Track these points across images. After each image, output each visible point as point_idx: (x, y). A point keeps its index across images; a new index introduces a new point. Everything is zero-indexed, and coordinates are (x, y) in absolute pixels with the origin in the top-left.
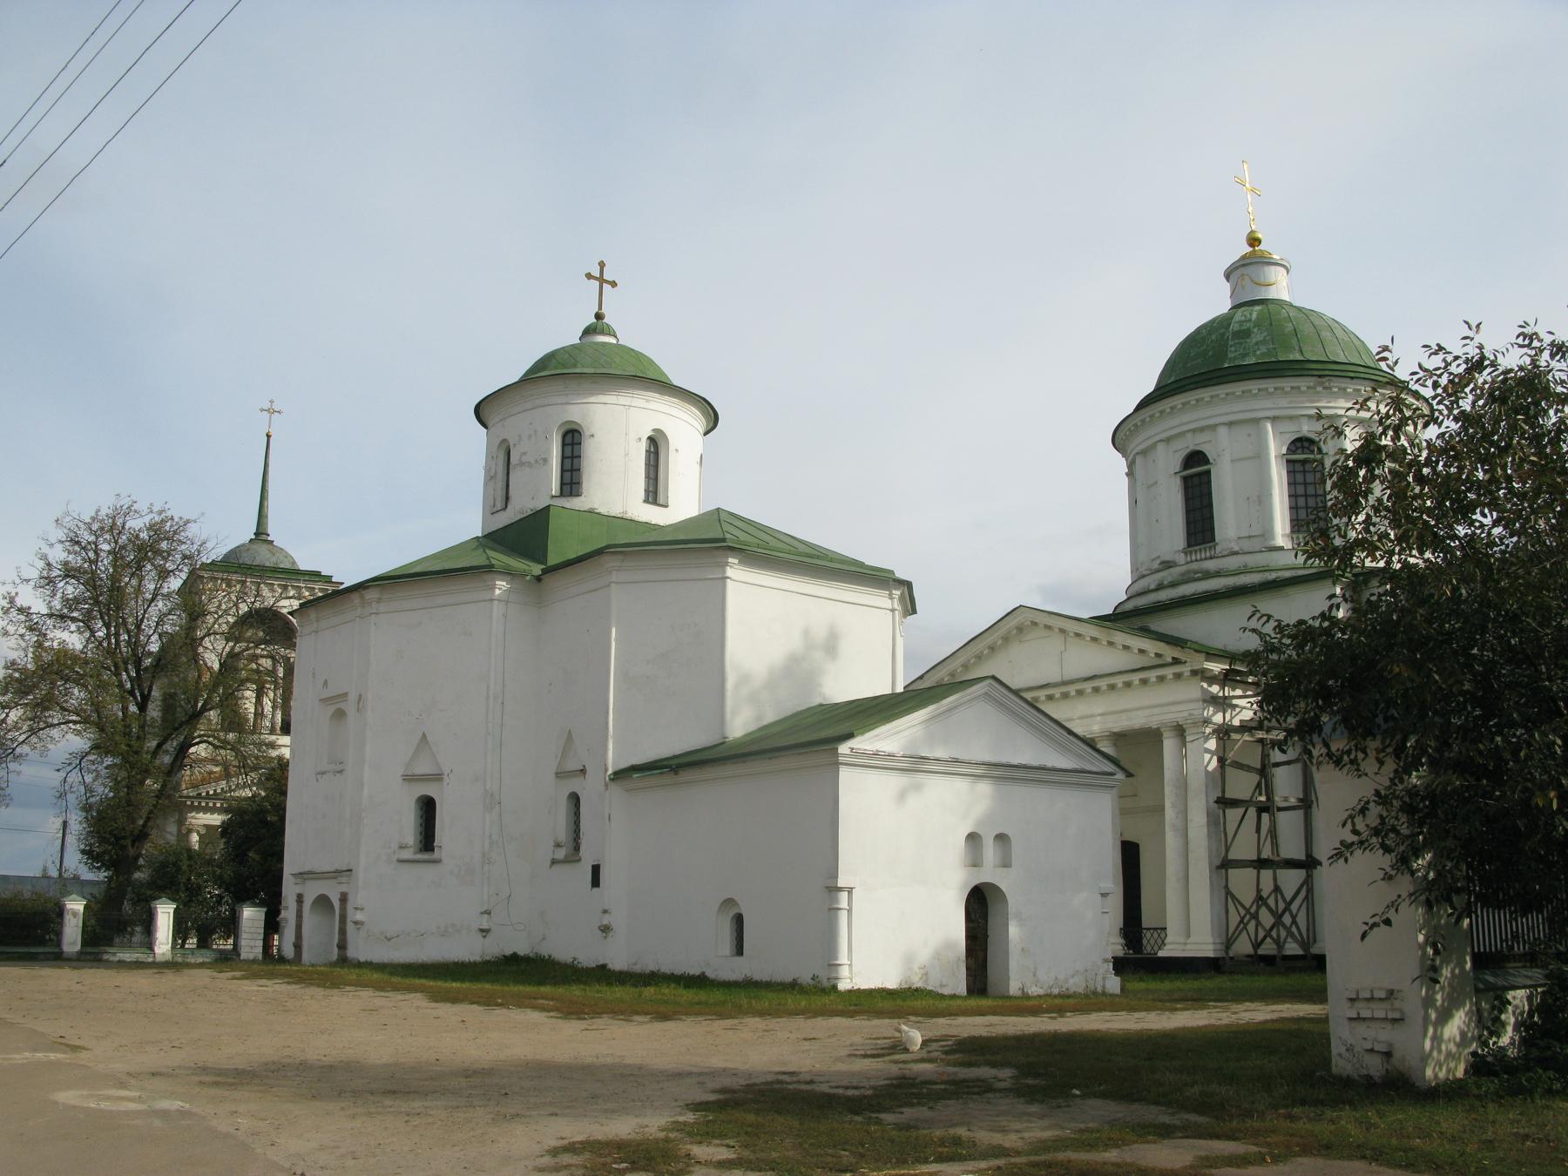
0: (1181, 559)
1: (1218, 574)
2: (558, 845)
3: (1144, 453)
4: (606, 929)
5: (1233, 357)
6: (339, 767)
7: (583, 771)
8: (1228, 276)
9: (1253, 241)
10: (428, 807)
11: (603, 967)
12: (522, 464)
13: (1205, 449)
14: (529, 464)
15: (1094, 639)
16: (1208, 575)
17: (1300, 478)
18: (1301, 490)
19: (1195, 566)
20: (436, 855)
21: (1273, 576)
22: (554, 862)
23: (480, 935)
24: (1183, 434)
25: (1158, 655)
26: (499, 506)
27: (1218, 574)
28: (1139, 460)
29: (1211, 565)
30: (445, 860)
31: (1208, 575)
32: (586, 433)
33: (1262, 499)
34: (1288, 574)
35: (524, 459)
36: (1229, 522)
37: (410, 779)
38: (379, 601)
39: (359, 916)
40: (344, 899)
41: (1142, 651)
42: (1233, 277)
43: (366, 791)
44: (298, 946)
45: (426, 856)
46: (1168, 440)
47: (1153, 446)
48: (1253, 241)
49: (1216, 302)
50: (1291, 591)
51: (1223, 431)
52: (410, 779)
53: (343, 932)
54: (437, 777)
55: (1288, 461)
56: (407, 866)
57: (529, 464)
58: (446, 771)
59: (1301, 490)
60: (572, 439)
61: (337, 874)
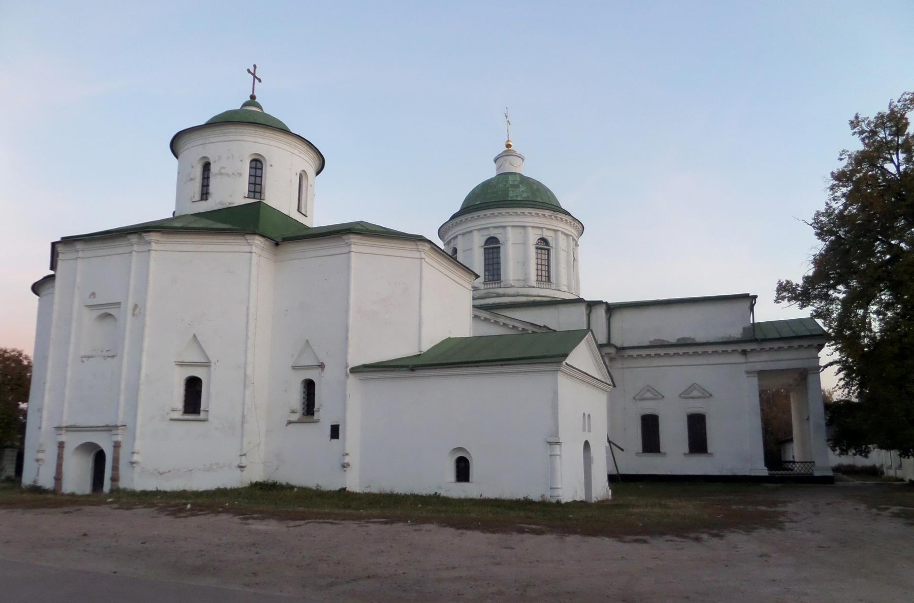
0: (482, 287)
1: (504, 295)
2: (293, 412)
3: (463, 234)
4: (345, 466)
5: (512, 195)
6: (109, 354)
7: (322, 366)
8: (495, 161)
9: (508, 146)
10: (193, 387)
11: (344, 489)
12: (221, 174)
13: (498, 236)
14: (228, 175)
15: (486, 319)
16: (499, 295)
17: (539, 256)
18: (539, 262)
19: (492, 290)
20: (202, 415)
21: (532, 299)
22: (290, 423)
23: (239, 470)
24: (488, 228)
25: (523, 329)
26: (197, 197)
27: (504, 295)
28: (459, 237)
29: (501, 291)
30: (210, 418)
31: (499, 295)
32: (268, 163)
33: (525, 263)
34: (524, 299)
35: (223, 171)
36: (511, 270)
37: (182, 364)
38: (157, 242)
39: (136, 458)
40: (117, 446)
41: (514, 327)
42: (500, 161)
43: (143, 371)
44: (58, 478)
45: (187, 417)
46: (479, 230)
47: (471, 231)
48: (508, 146)
49: (490, 172)
50: (559, 306)
51: (530, 229)
52: (182, 364)
53: (115, 468)
54: (207, 365)
55: (537, 248)
56: (175, 423)
57: (228, 175)
58: (213, 360)
59: (539, 262)
60: (257, 164)
61: (110, 429)
